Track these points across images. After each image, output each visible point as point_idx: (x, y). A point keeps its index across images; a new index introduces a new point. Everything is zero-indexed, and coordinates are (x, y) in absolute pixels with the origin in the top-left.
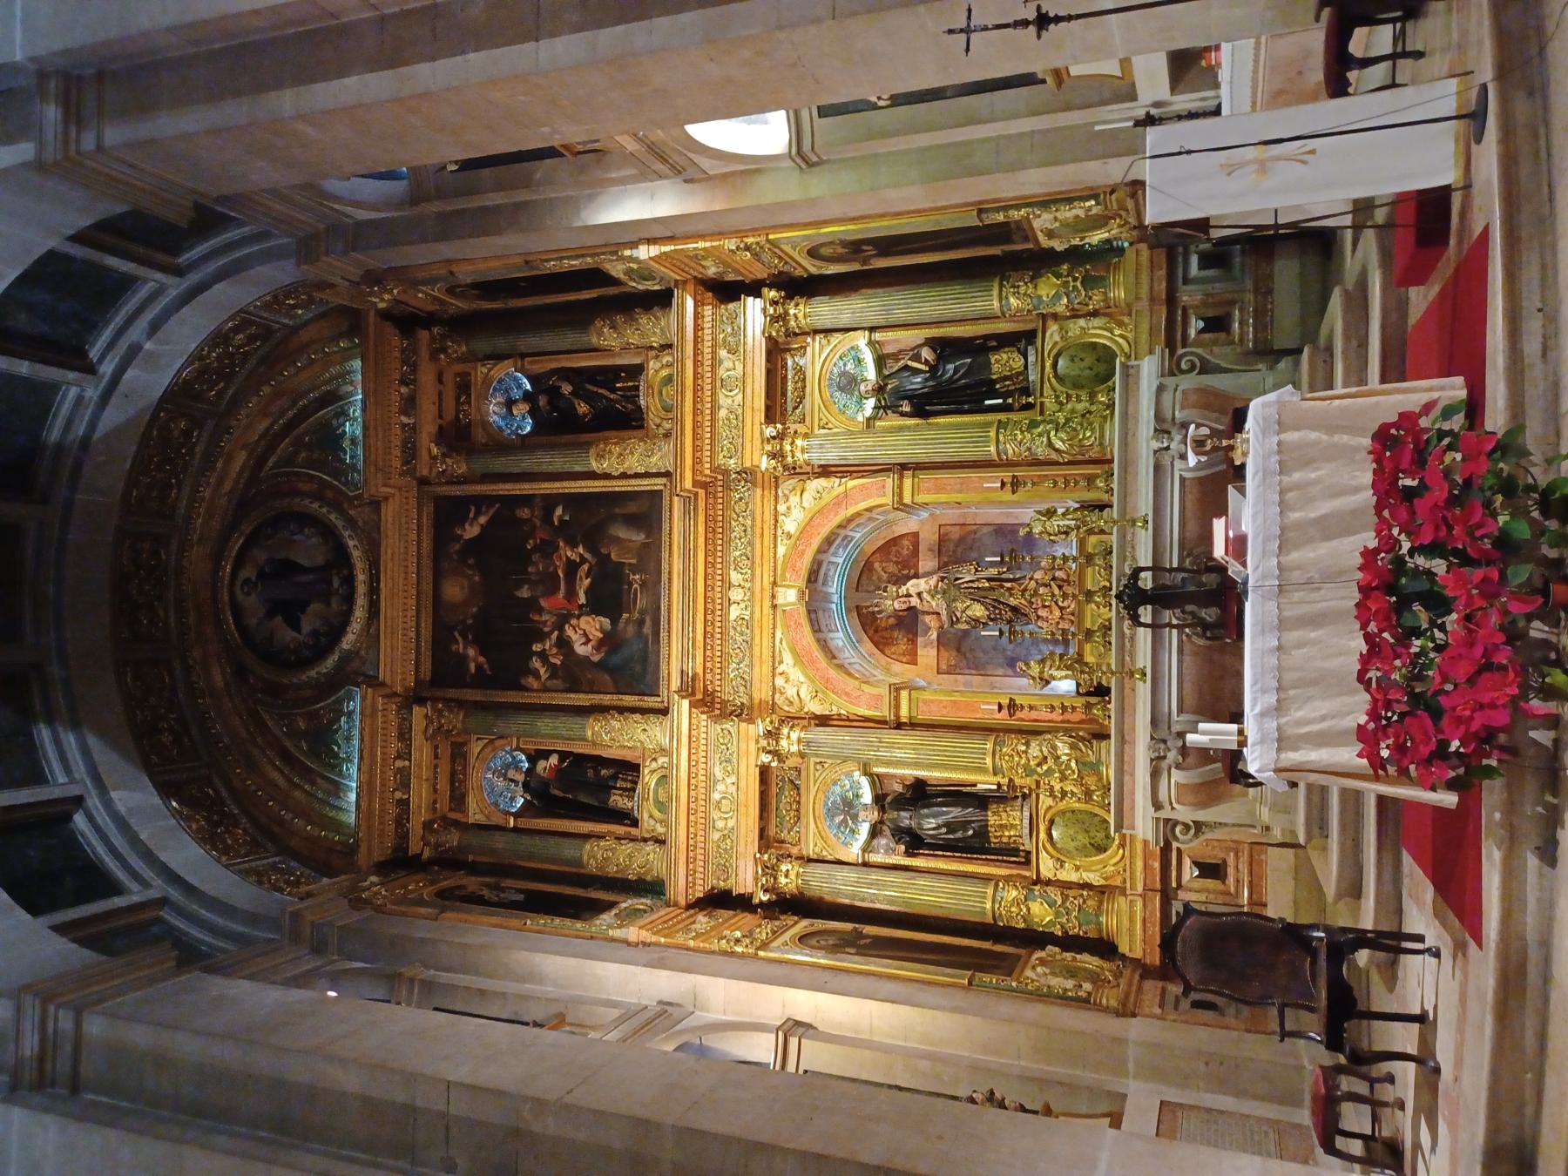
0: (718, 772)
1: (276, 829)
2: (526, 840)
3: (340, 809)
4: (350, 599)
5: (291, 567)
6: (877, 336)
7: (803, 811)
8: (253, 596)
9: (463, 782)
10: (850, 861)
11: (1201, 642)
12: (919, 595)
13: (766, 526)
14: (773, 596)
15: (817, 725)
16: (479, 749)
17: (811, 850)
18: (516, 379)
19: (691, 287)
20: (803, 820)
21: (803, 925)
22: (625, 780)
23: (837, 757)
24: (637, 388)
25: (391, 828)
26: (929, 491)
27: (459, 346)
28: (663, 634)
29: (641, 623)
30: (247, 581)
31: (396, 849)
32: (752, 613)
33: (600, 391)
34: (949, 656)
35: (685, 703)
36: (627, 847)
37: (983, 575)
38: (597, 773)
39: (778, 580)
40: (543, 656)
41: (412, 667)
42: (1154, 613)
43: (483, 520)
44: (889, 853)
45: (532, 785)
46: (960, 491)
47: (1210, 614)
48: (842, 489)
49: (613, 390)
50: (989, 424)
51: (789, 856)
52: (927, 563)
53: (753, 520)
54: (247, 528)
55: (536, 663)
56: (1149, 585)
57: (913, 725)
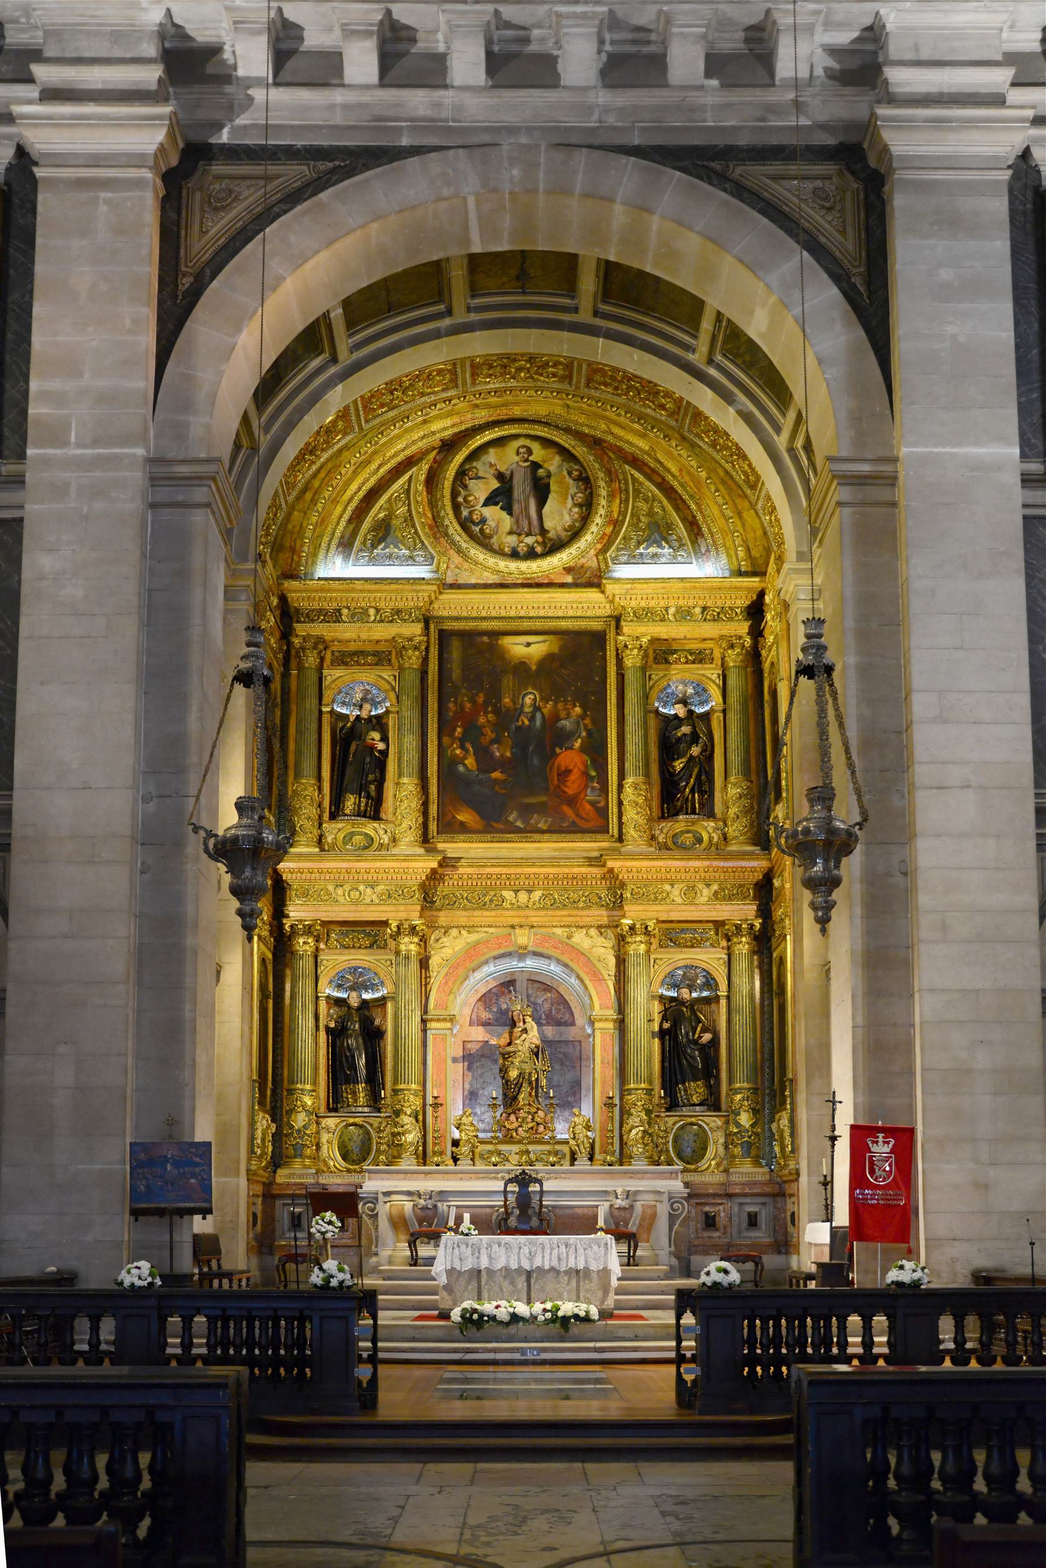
0: (380, 888)
1: (308, 496)
2: (314, 726)
3: (327, 551)
4: (515, 555)
5: (541, 491)
6: (723, 1002)
7: (352, 951)
8: (517, 459)
9: (358, 663)
10: (319, 987)
11: (494, 1217)
13: (578, 919)
14: (521, 926)
15: (421, 961)
16: (387, 677)
17: (321, 957)
18: (706, 702)
20: (346, 951)
22: (366, 805)
23: (398, 979)
24: (694, 812)
25: (316, 606)
26: (603, 1040)
27: (735, 661)
28: (489, 837)
30: (530, 452)
31: (297, 610)
32: (507, 909)
33: (692, 780)
36: (314, 812)
37: (541, 1076)
38: (371, 782)
39: (535, 930)
41: (455, 614)
42: (513, 1192)
44: (327, 1016)
45: (358, 725)
46: (602, 1062)
47: (513, 1222)
48: (607, 977)
49: (692, 791)
50: (650, 1082)
53: (583, 909)
54: (580, 451)
56: (530, 1189)
57: (424, 1031)
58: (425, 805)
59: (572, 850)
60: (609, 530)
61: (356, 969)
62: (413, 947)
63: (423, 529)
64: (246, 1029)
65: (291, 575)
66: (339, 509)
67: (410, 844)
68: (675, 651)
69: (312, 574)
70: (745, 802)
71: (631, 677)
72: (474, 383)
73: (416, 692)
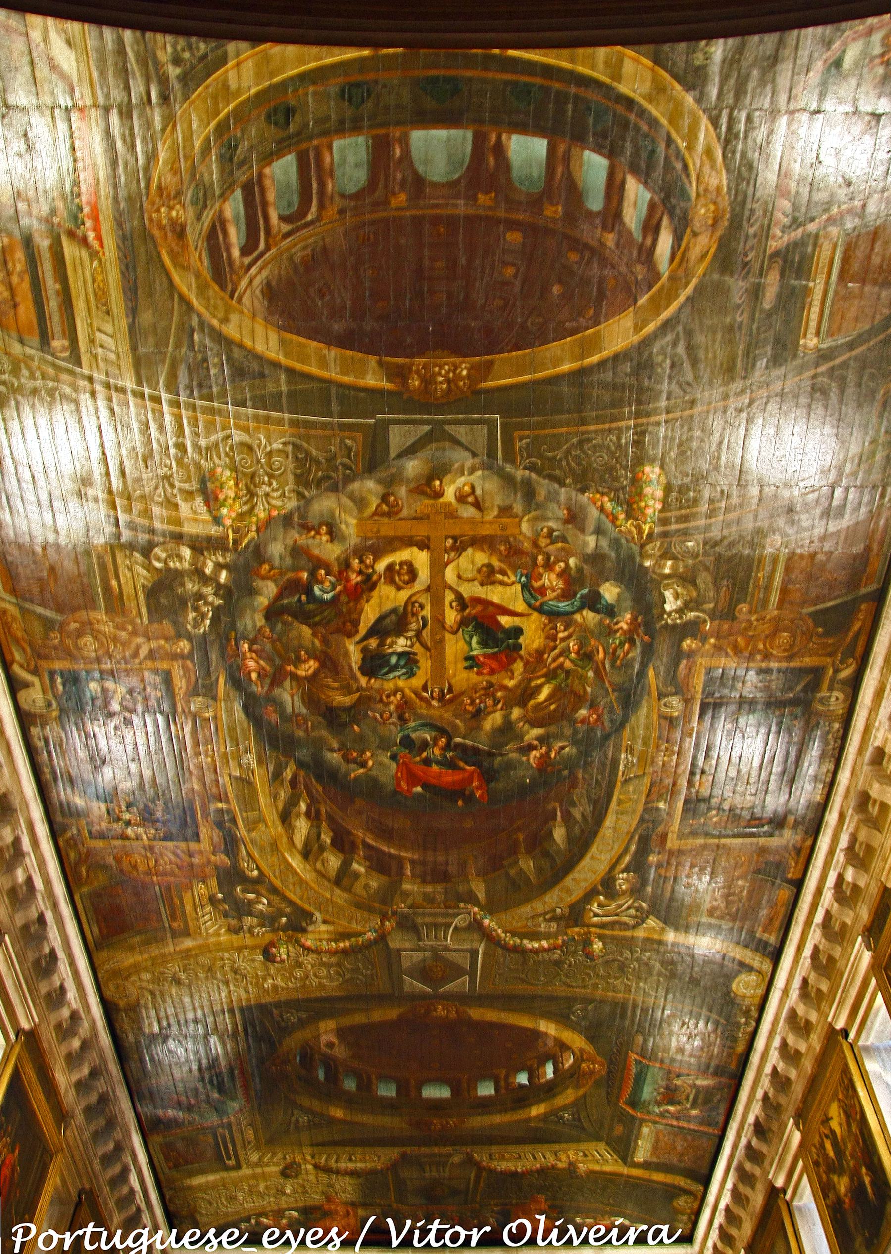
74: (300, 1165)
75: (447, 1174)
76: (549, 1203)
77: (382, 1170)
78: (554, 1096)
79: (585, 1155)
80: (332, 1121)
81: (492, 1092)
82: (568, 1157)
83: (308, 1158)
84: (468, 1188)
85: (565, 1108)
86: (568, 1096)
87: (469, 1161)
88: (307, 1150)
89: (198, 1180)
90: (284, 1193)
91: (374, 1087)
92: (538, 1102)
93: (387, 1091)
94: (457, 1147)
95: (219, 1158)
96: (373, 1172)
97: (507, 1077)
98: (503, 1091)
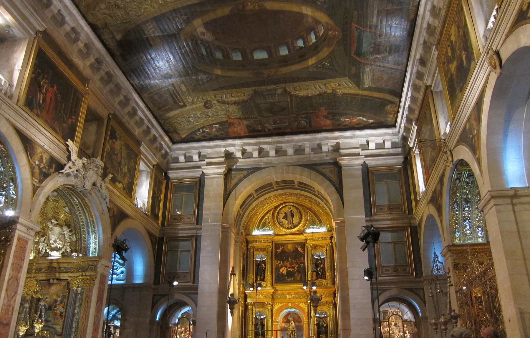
0: (264, 296)
1: (251, 219)
4: (288, 228)
5: (293, 216)
12: (292, 324)
14: (290, 302)
19: (334, 289)
21: (244, 309)
24: (322, 278)
29: (285, 280)
30: (290, 208)
34: (283, 327)
35: (273, 291)
40: (280, 263)
43: (301, 251)
49: (321, 274)
51: (252, 306)
52: (297, 324)
54: (299, 208)
55: (279, 262)
57: (272, 324)
58: (272, 278)
59: (299, 286)
60: (305, 223)
61: (260, 312)
62: (270, 307)
63: (271, 223)
64: (238, 326)
65: (248, 235)
66: (257, 221)
67: (269, 287)
68: (317, 246)
69: (252, 234)
70: (331, 276)
71: (309, 252)
72: (280, 196)
73: (270, 256)
74: (210, 101)
75: (277, 100)
76: (327, 111)
77: (247, 101)
78: (318, 53)
79: (339, 85)
80: (217, 76)
81: (288, 53)
82: (331, 87)
83: (213, 97)
84: (288, 106)
85: (324, 59)
86: (325, 52)
87: (285, 92)
88: (211, 93)
89: (171, 114)
90: (209, 116)
91: (231, 56)
92: (311, 57)
93: (237, 57)
94: (278, 85)
95: (175, 102)
96: (243, 102)
97: (293, 44)
98: (292, 52)
